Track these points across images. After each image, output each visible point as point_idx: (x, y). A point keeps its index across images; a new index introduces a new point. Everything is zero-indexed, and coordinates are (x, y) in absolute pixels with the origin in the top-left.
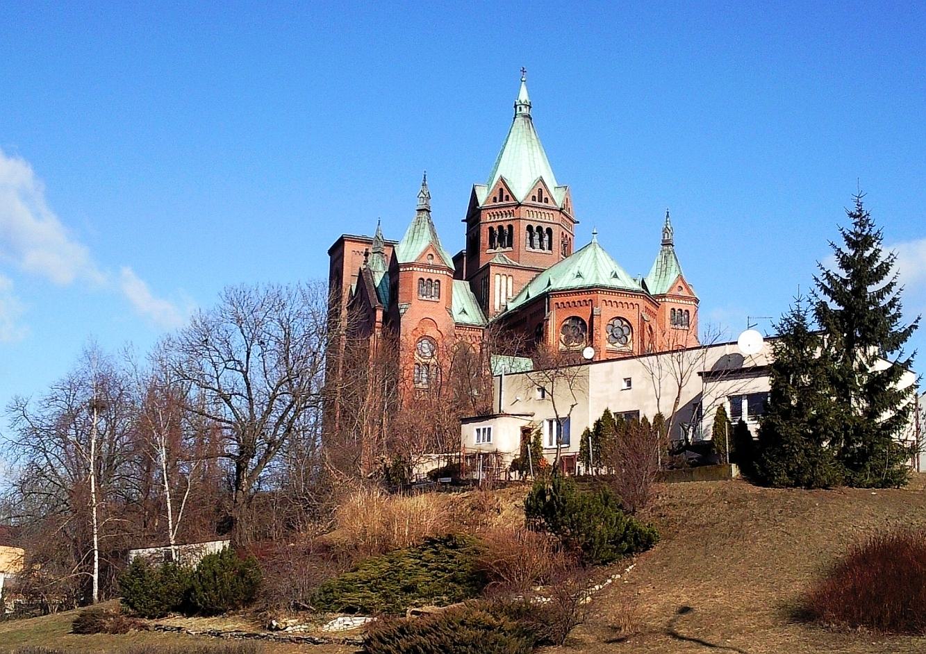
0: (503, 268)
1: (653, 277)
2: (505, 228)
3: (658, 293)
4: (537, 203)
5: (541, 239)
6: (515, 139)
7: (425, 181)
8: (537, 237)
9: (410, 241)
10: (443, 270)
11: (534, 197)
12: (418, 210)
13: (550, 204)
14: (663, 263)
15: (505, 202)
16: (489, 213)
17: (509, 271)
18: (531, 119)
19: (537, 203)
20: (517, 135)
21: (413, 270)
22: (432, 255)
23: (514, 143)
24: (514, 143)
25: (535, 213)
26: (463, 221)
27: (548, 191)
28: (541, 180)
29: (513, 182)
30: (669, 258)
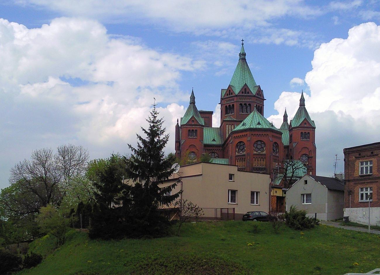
5: (247, 108)
8: (245, 107)
9: (187, 115)
11: (243, 93)
21: (187, 127)
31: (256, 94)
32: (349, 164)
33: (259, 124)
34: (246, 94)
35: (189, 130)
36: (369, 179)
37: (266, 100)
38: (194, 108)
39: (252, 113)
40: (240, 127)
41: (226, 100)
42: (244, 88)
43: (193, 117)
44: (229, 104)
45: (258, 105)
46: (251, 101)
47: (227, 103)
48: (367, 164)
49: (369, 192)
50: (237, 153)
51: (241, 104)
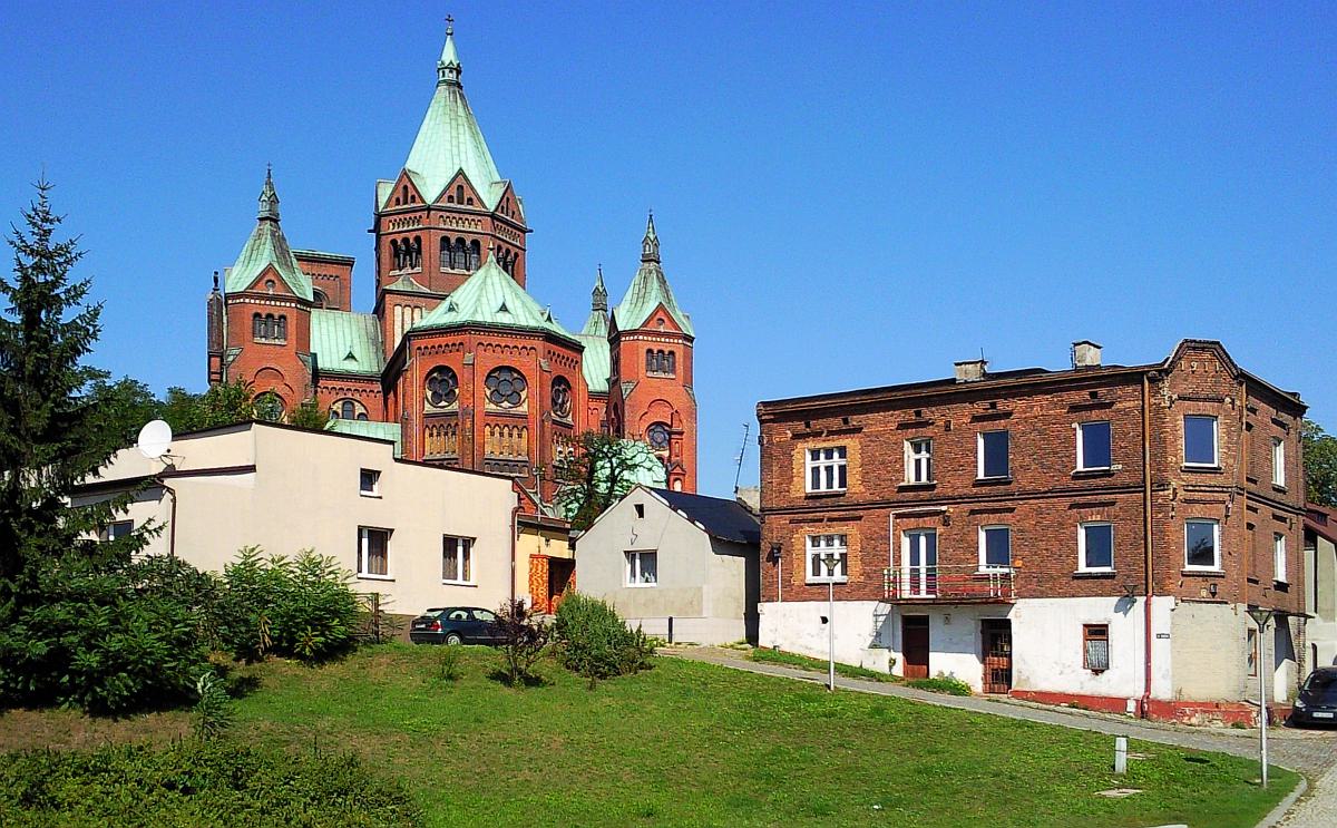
1: (627, 306)
2: (411, 241)
7: (269, 177)
9: (246, 262)
10: (291, 301)
11: (451, 199)
12: (260, 219)
18: (460, 87)
22: (273, 282)
23: (433, 122)
24: (433, 122)
26: (369, 231)
27: (472, 188)
28: (461, 172)
31: (496, 210)
32: (774, 460)
33: (504, 308)
34: (462, 206)
35: (257, 315)
36: (838, 508)
37: (531, 231)
38: (273, 234)
39: (481, 271)
40: (438, 316)
41: (392, 218)
42: (455, 185)
43: (270, 268)
45: (505, 246)
46: (479, 229)
47: (396, 230)
48: (829, 455)
49: (837, 549)
50: (427, 405)
51: (445, 240)
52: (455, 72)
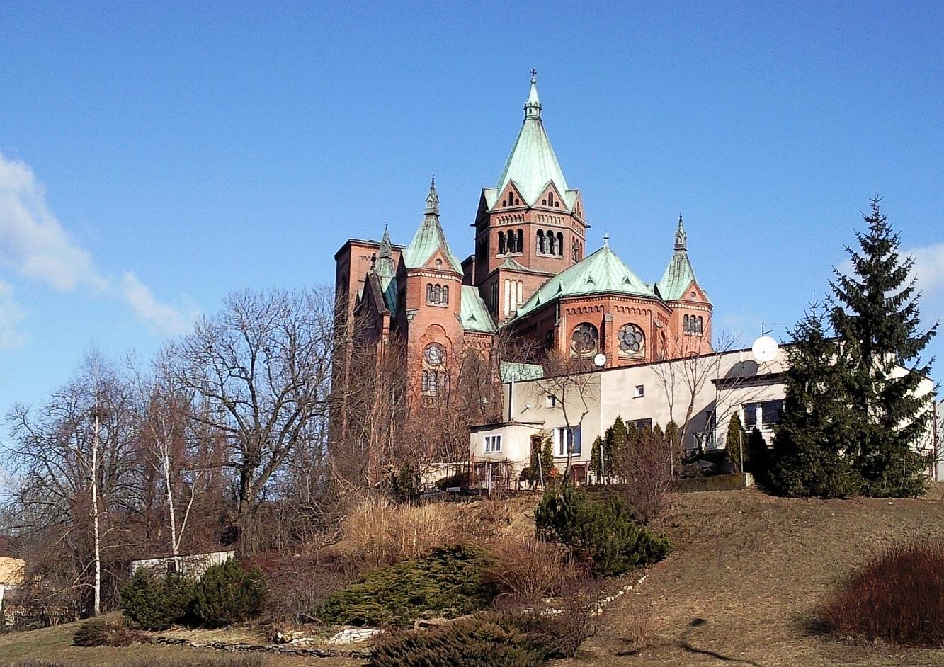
0: (513, 274)
1: (666, 283)
2: (514, 233)
3: (671, 299)
4: (547, 207)
5: (551, 244)
6: (525, 142)
8: (547, 242)
9: (418, 246)
10: (451, 275)
11: (544, 201)
12: (426, 214)
13: (561, 208)
14: (676, 268)
15: (515, 206)
16: (498, 218)
17: (519, 277)
18: (541, 121)
19: (547, 207)
20: (528, 138)
21: (421, 275)
22: (440, 260)
24: (524, 146)
25: (550, 218)
26: (472, 225)
27: (559, 195)
28: (552, 183)
29: (523, 185)
30: (682, 264)
44: (509, 228)
52: (538, 110)
